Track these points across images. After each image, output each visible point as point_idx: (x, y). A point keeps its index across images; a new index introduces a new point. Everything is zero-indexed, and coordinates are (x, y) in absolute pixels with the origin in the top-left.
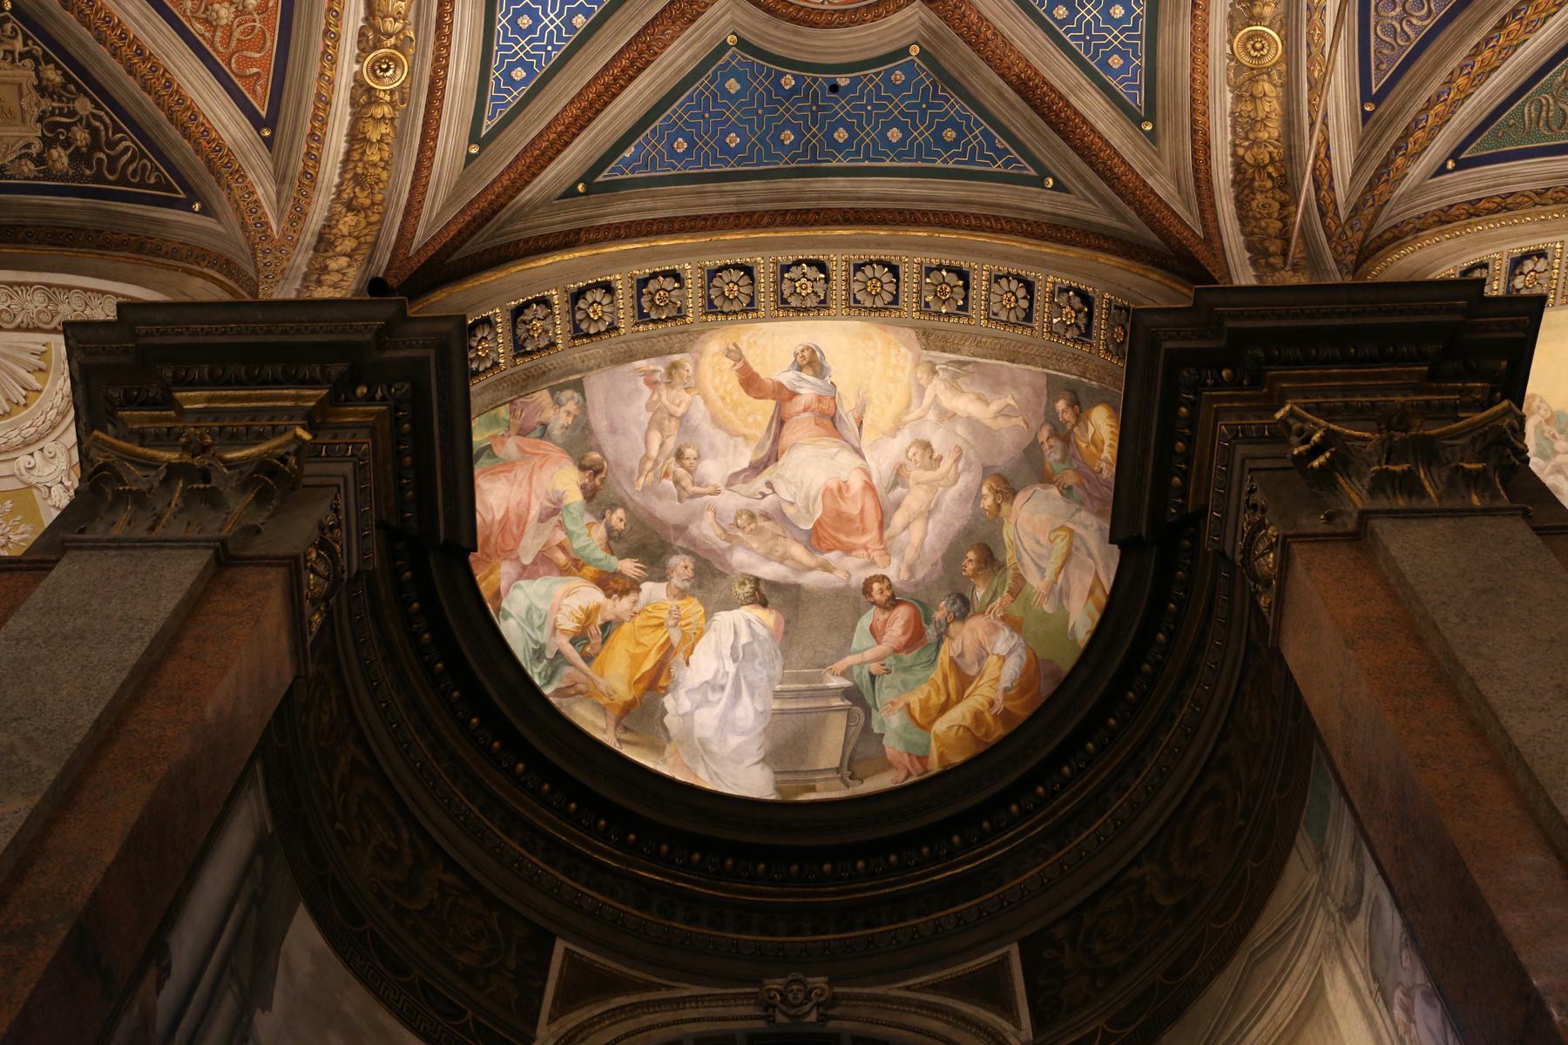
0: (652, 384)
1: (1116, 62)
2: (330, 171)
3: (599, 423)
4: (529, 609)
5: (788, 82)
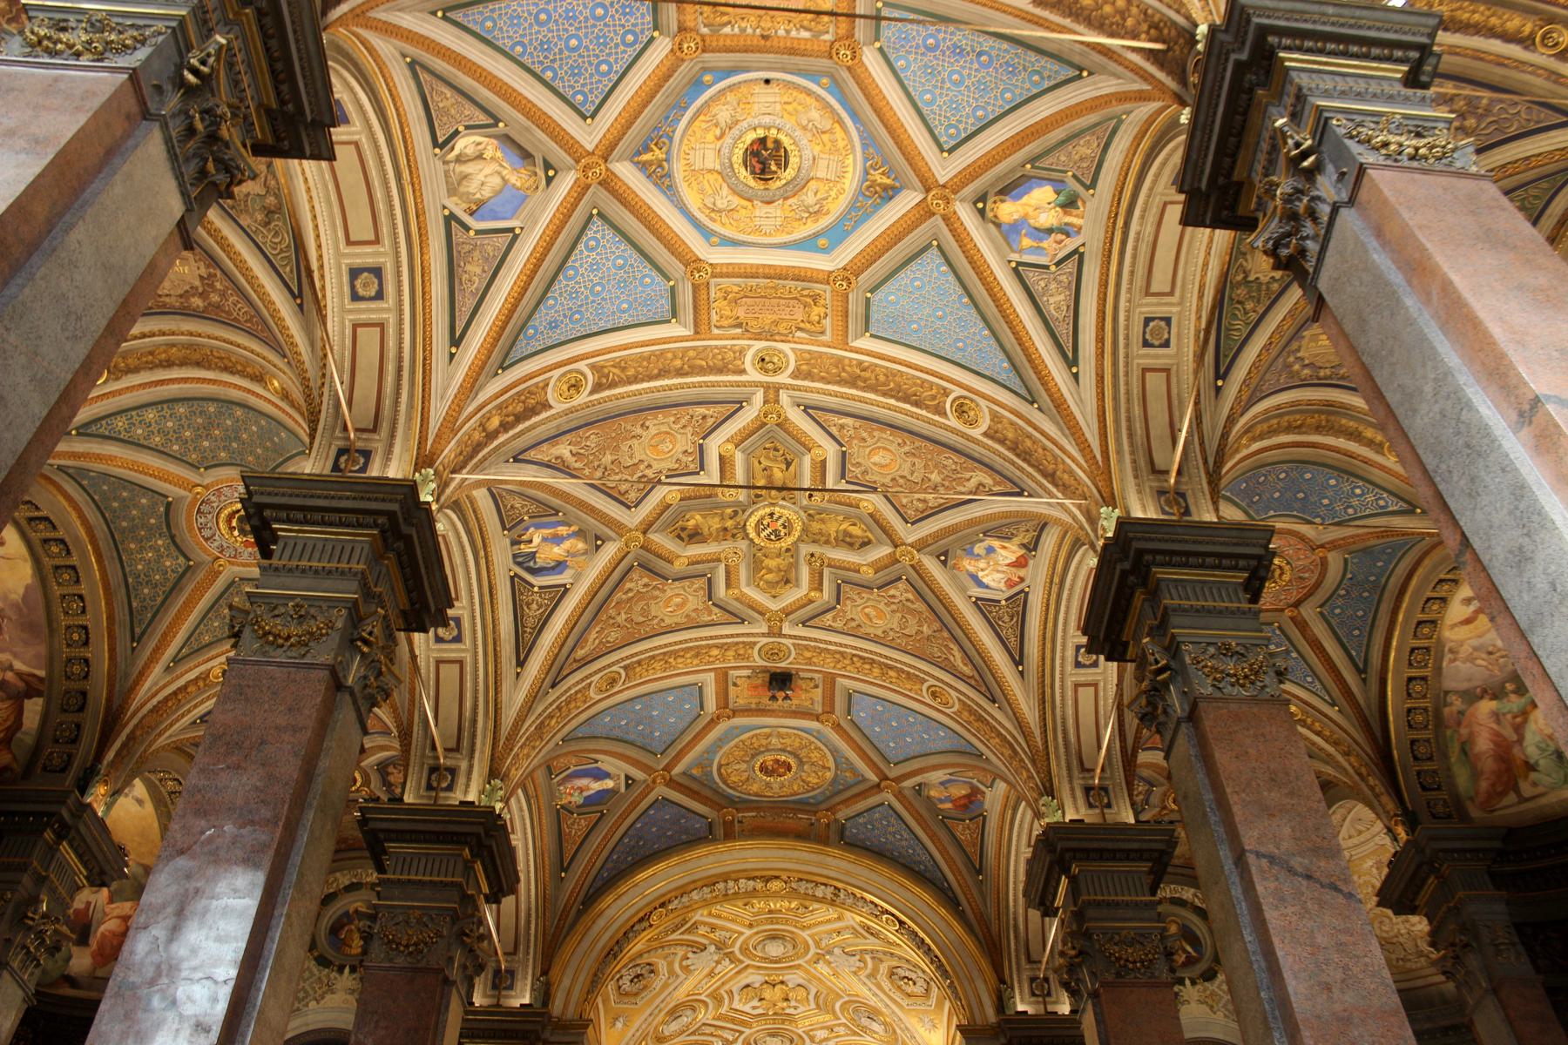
0: (1455, 660)
1: (1382, 503)
2: (1330, 749)
3: (1464, 686)
4: (1538, 747)
5: (1342, 592)
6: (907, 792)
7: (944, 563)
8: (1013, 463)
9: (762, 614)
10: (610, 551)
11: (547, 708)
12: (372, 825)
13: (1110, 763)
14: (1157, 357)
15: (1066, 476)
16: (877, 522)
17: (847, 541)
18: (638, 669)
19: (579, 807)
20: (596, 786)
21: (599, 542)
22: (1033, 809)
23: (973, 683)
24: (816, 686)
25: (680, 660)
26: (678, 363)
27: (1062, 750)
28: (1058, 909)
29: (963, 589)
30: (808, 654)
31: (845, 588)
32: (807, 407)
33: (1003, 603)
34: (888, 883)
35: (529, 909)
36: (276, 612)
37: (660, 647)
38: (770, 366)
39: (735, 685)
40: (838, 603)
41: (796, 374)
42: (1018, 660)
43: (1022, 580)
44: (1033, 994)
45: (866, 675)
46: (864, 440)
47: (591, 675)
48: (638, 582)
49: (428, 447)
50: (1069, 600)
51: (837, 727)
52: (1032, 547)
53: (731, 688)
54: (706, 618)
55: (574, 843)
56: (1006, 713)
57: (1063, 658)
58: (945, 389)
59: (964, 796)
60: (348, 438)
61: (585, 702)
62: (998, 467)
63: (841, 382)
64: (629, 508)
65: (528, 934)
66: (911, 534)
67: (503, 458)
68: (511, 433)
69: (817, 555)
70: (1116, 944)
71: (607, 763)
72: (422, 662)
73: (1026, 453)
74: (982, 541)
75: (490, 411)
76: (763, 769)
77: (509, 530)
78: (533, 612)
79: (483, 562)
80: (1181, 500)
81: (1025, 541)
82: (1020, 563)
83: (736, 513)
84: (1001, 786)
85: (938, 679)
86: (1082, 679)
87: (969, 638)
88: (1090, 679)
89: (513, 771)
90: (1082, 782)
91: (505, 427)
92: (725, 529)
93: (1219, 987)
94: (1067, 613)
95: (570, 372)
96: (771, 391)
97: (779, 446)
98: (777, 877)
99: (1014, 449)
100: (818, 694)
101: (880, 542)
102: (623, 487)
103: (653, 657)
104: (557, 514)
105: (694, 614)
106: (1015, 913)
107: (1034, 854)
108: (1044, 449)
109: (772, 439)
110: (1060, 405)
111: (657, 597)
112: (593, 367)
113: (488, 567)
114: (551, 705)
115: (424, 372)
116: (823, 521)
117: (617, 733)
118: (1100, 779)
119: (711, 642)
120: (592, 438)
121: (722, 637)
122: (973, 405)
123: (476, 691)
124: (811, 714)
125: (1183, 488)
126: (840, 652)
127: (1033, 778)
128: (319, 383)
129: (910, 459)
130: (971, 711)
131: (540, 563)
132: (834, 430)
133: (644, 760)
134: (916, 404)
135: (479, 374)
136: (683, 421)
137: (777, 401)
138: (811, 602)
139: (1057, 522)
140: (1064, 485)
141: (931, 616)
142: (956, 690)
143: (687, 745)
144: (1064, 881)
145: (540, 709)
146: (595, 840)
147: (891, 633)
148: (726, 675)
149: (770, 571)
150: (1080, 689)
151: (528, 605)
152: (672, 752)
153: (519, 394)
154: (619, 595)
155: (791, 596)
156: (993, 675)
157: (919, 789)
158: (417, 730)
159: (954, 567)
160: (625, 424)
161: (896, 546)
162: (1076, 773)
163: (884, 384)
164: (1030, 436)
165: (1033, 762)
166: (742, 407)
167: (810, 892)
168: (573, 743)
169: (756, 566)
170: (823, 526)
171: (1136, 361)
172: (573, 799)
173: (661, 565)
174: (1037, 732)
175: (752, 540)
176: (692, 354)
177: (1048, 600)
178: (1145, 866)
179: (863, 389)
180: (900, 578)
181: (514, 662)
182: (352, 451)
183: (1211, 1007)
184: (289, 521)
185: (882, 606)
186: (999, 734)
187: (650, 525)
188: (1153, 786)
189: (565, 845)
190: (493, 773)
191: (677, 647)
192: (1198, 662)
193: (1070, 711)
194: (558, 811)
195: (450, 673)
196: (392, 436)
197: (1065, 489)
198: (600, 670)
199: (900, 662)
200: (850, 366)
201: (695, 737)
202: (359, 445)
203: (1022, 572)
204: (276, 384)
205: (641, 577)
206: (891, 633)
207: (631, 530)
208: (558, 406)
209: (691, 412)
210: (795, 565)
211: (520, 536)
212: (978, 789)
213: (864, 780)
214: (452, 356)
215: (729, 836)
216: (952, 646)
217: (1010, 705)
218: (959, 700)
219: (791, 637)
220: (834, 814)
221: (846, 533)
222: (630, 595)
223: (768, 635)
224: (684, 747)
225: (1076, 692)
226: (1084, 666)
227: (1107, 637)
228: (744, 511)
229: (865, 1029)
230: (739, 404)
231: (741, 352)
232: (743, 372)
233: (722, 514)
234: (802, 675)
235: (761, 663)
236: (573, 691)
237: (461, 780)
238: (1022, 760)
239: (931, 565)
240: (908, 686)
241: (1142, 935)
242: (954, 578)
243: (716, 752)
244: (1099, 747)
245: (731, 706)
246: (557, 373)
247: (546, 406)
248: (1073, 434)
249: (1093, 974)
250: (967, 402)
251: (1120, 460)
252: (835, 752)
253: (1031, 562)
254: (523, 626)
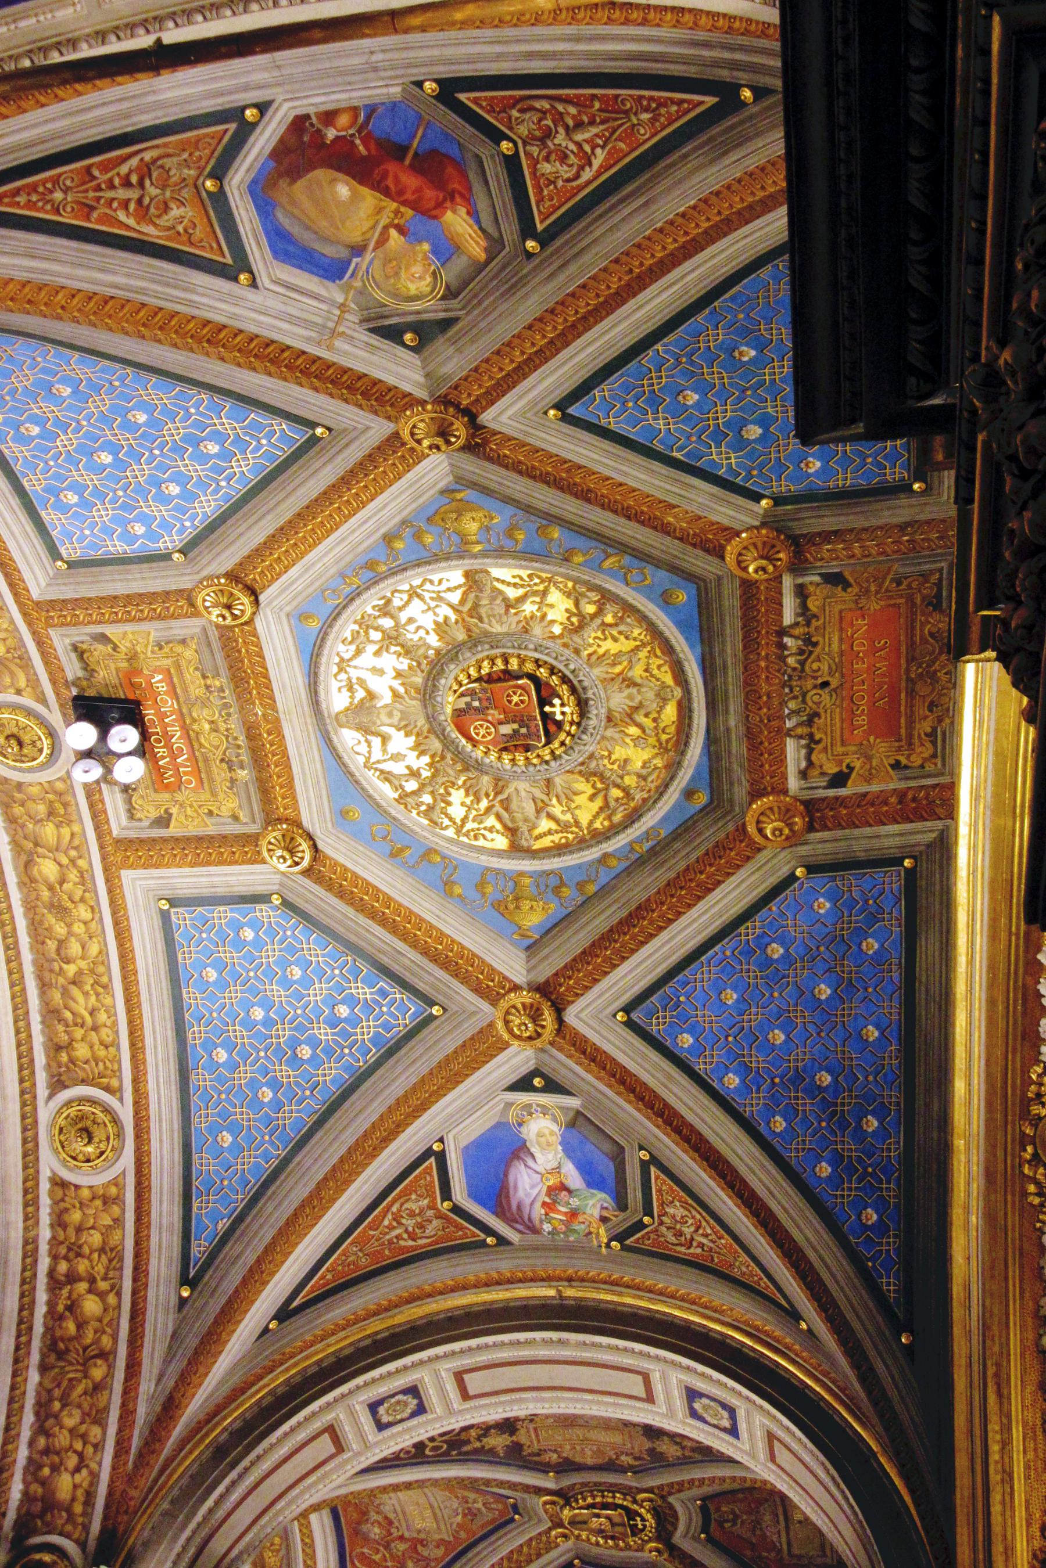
19: (622, 1205)
25: (74, 948)
39: (164, 821)
53: (173, 830)
143: (404, 937)
148: (125, 844)
189: (736, 1273)
191: (27, 957)
212: (280, 152)
224: (414, 944)
234: (72, 669)
236: (45, 1233)
245: (253, 829)
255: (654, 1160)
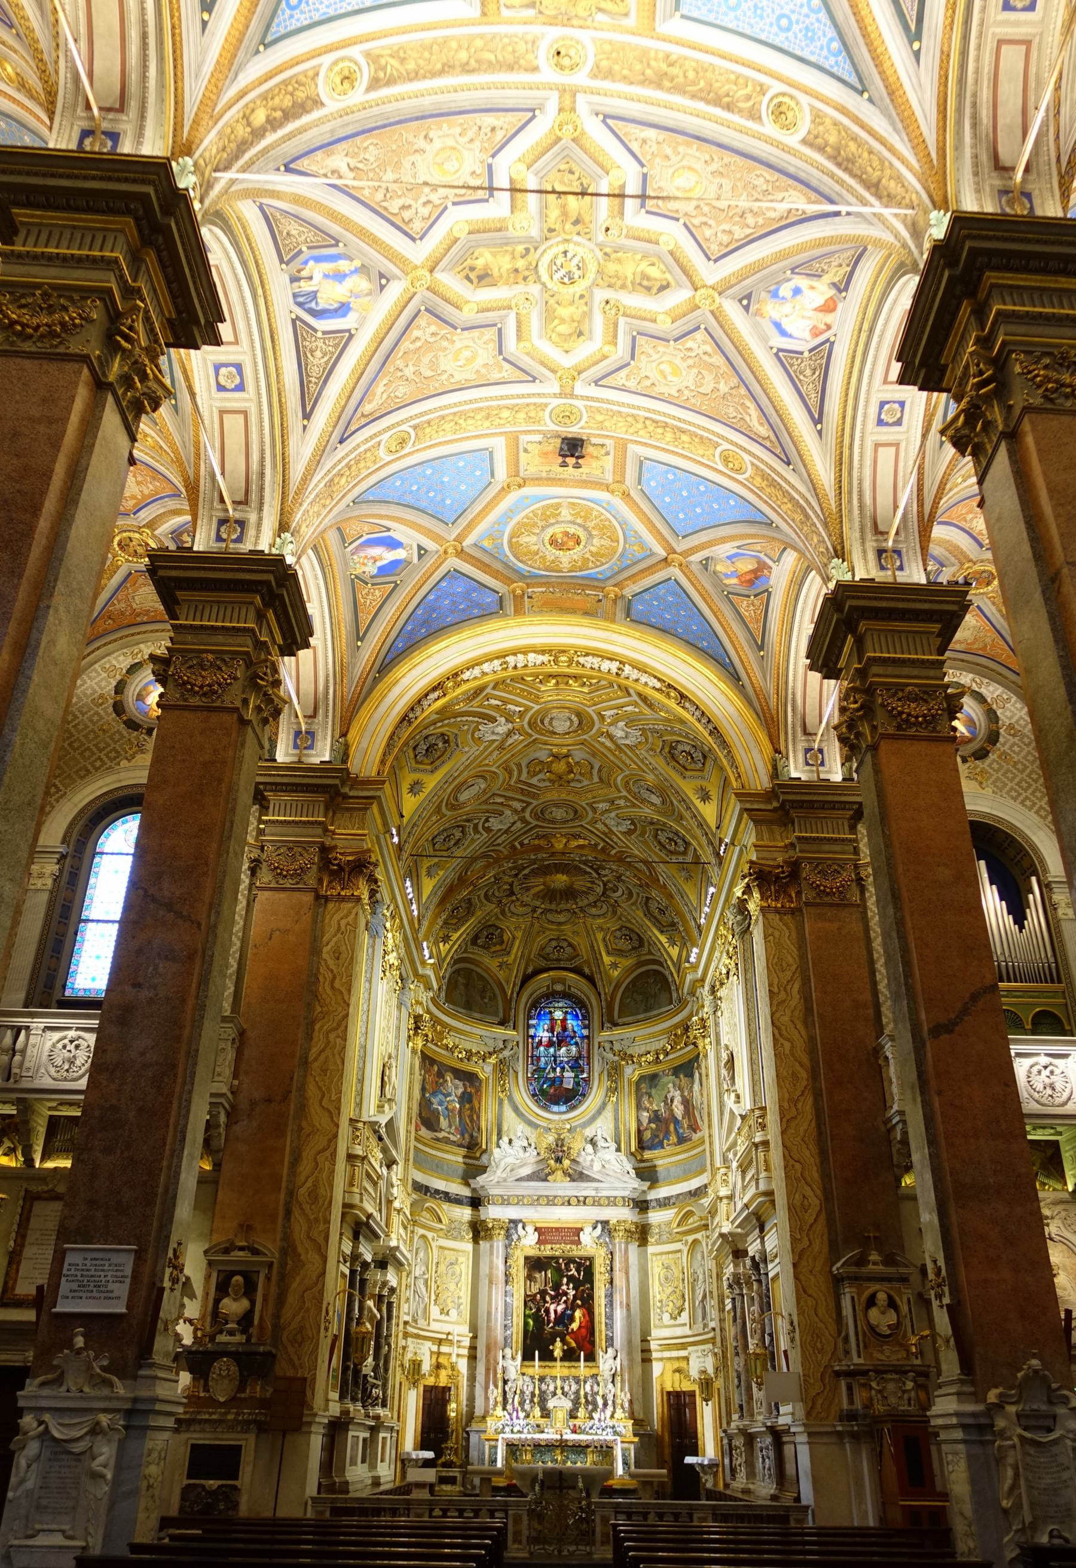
6: (693, 567)
7: (747, 308)
8: (832, 176)
9: (554, 371)
10: (395, 290)
11: (335, 465)
12: (161, 573)
13: (906, 527)
14: (1017, 24)
15: (892, 184)
16: (677, 261)
17: (646, 286)
18: (428, 430)
20: (390, 556)
21: (384, 281)
22: (821, 575)
23: (768, 444)
24: (607, 454)
25: (470, 422)
26: (463, 55)
27: (856, 512)
28: (841, 670)
29: (764, 339)
30: (600, 418)
31: (641, 340)
32: (606, 117)
33: (806, 354)
34: (671, 659)
35: (327, 676)
36: (23, 301)
37: (450, 406)
38: (566, 62)
39: (526, 451)
40: (633, 358)
41: (598, 73)
42: (818, 419)
43: (829, 327)
44: (807, 764)
45: (658, 440)
46: (667, 157)
47: (380, 433)
48: (425, 328)
49: (185, 135)
50: (877, 349)
51: (626, 496)
52: (843, 287)
53: (522, 454)
54: (496, 376)
55: (369, 613)
56: (800, 476)
57: (865, 415)
58: (761, 85)
59: (752, 571)
60: (92, 118)
61: (375, 462)
62: (814, 183)
63: (645, 82)
64: (414, 240)
65: (327, 699)
66: (711, 274)
67: (272, 165)
68: (280, 133)
69: (612, 303)
70: (899, 700)
71: (399, 532)
72: (205, 414)
73: (848, 160)
74: (789, 280)
75: (253, 101)
76: (553, 542)
77: (287, 264)
78: (317, 362)
79: (261, 301)
80: (1026, 201)
81: (836, 280)
82: (829, 307)
83: (527, 250)
84: (790, 558)
85: (732, 443)
86: (883, 438)
87: (767, 394)
88: (891, 438)
89: (304, 528)
90: (875, 544)
91: (273, 124)
92: (516, 271)
93: (990, 765)
94: (874, 364)
95: (342, 59)
96: (567, 96)
97: (575, 168)
98: (564, 651)
99: (834, 158)
100: (608, 462)
101: (679, 285)
102: (407, 215)
103: (443, 417)
104: (337, 245)
105: (483, 371)
106: (794, 688)
107: (816, 629)
108: (870, 152)
109: (567, 160)
110: (893, 91)
111: (445, 349)
112: (368, 55)
113: (267, 308)
114: (340, 461)
115: (174, 44)
116: (619, 261)
117: (409, 499)
118: (894, 541)
119: (502, 402)
120: (371, 149)
121: (513, 397)
122: (792, 104)
123: (262, 443)
124: (602, 484)
125: (1029, 187)
126: (633, 416)
127: (824, 542)
128: (54, 55)
129: (718, 180)
130: (764, 476)
131: (322, 305)
132: (635, 147)
133: (437, 530)
134: (728, 107)
135: (237, 49)
136: (470, 134)
137: (573, 110)
138: (605, 357)
139: (878, 243)
140: (889, 196)
141: (730, 371)
142: (749, 453)
143: (478, 515)
144: (850, 639)
145: (328, 465)
146: (390, 612)
147: (686, 392)
148: (517, 439)
149: (563, 321)
150: (880, 449)
151: (312, 351)
152: (463, 523)
153: (286, 83)
154: (406, 345)
155: (584, 350)
156: (789, 434)
157: (706, 563)
158: (204, 484)
159: (759, 313)
160: (407, 133)
161: (696, 290)
162: (869, 536)
163: (694, 83)
164: (855, 138)
165: (826, 525)
166: (534, 117)
167: (596, 666)
168: (364, 506)
169: (549, 315)
170: (618, 267)
171: (991, 31)
172: (367, 569)
173: (448, 310)
174: (832, 495)
175: (544, 284)
176: (479, 43)
177: (855, 352)
178: (936, 627)
179: (669, 90)
180: (698, 328)
181: (300, 414)
182: (98, 133)
183: (981, 783)
184: (29, 205)
185: (678, 361)
186: (792, 499)
187: (437, 264)
188: (943, 565)
189: (360, 615)
190: (283, 527)
191: (467, 407)
192: (1030, 372)
193: (868, 473)
194: (352, 581)
195: (233, 423)
196: (142, 116)
197: (888, 199)
198: (389, 428)
199: (694, 425)
200: (656, 60)
201: (486, 506)
202: (105, 126)
203: (829, 318)
204: (9, 69)
205: (429, 324)
206: (686, 392)
207: (416, 267)
208: (332, 105)
209: (479, 123)
210: (588, 315)
211: (299, 271)
213: (652, 554)
214: (204, 24)
215: (519, 611)
216: (748, 404)
217: (805, 466)
218: (753, 464)
219: (583, 398)
220: (621, 589)
221: (645, 276)
222: (418, 344)
223: (561, 395)
225: (876, 451)
226: (887, 424)
227: (922, 363)
228: (536, 249)
229: (644, 801)
230: (533, 112)
231: (534, 42)
232: (535, 69)
233: (513, 253)
234: (594, 440)
235: (553, 427)
236: (361, 449)
237: (251, 532)
238: (814, 524)
239: (732, 310)
240: (701, 452)
241: (926, 693)
242: (756, 326)
243: (506, 524)
244: (896, 507)
245: (521, 474)
246: (327, 59)
247: (318, 103)
248: (905, 128)
249: (874, 728)
250: (786, 99)
251: (957, 158)
252: (623, 524)
253: (840, 306)
254: (308, 376)
255: (397, 585)
